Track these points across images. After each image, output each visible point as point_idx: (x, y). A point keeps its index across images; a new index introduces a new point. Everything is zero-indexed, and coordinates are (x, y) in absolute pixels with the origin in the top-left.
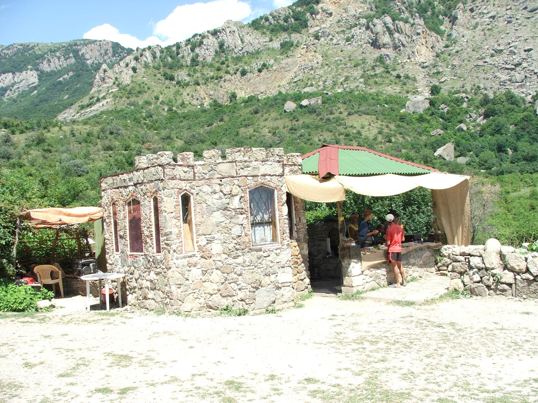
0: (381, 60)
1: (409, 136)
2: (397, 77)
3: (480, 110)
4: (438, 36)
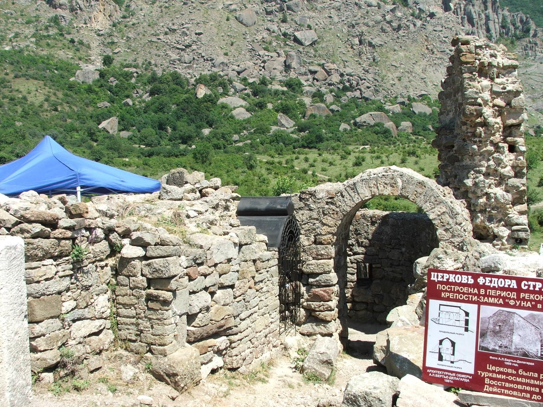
0: (56, 20)
1: (76, 106)
2: (70, 41)
3: (147, 87)
4: (117, 5)
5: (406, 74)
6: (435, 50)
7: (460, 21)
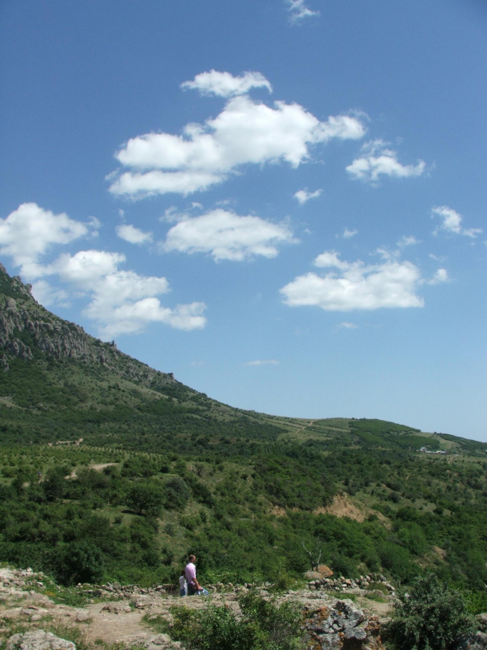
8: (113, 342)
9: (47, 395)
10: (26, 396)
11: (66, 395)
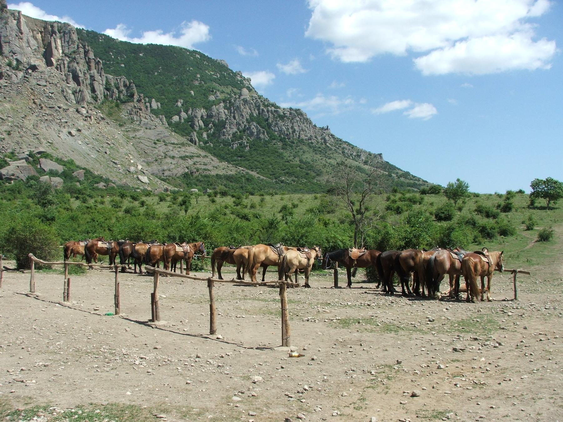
5: (16, 128)
6: (43, 105)
7: (65, 78)
8: (328, 127)
9: (287, 171)
10: (268, 171)
11: (304, 170)
